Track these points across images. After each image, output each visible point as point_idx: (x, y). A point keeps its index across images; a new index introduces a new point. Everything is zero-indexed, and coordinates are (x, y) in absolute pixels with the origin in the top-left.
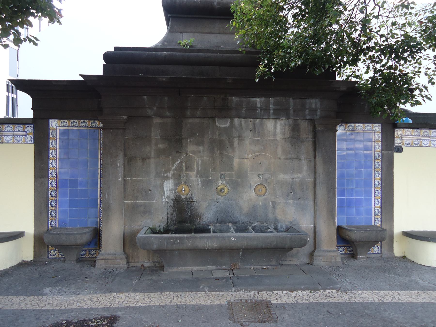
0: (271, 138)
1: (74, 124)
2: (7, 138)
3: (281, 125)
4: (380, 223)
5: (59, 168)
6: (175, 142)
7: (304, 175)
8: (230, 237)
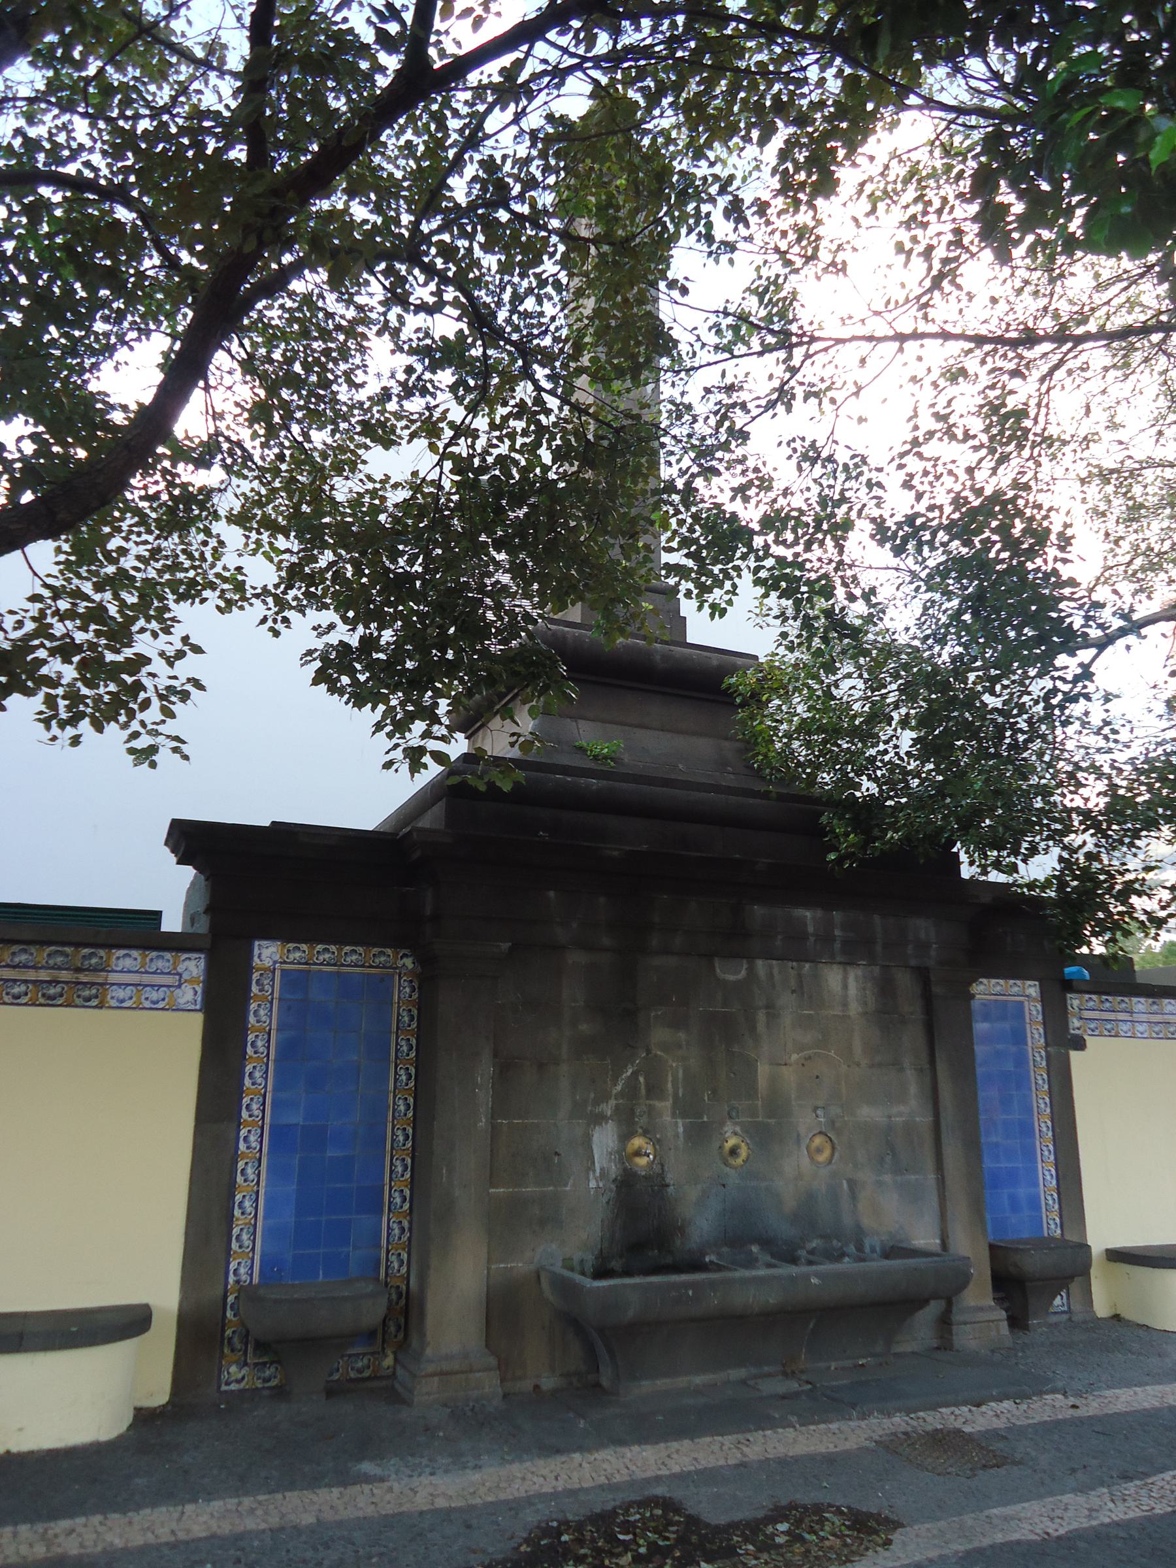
0: (837, 1011)
1: (327, 956)
2: (121, 993)
3: (856, 977)
4: (1059, 1231)
5: (275, 1090)
6: (620, 1018)
7: (910, 1109)
8: (807, 1277)
